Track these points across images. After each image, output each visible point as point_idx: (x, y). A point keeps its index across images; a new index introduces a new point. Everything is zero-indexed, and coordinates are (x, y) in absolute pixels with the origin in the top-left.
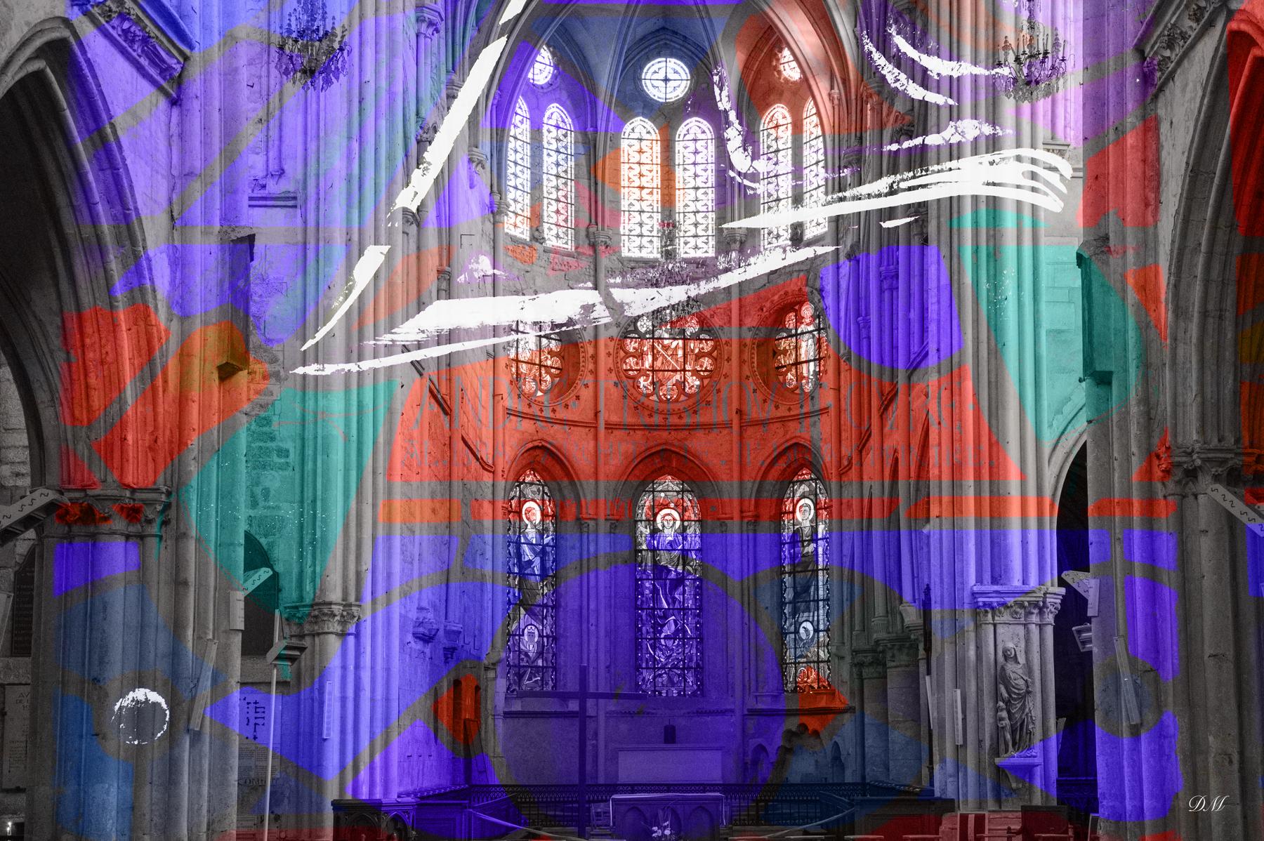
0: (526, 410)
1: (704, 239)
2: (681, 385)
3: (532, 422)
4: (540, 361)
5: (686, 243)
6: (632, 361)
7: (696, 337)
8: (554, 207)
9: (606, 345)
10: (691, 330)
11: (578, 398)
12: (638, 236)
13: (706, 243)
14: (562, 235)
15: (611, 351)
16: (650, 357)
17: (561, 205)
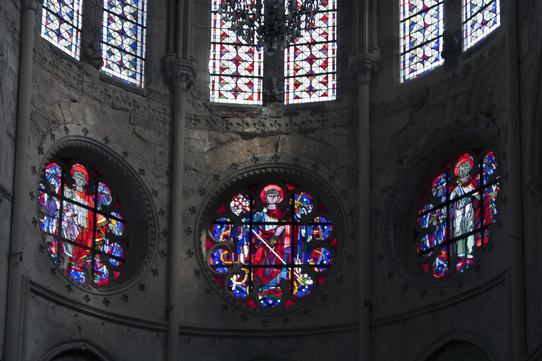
0: (64, 292)
1: (321, 78)
2: (290, 282)
3: (73, 313)
4: (94, 242)
5: (297, 85)
6: (222, 254)
7: (308, 221)
8: (117, 25)
9: (185, 219)
10: (304, 211)
11: (142, 287)
12: (232, 76)
13: (325, 83)
14: (127, 65)
15: (192, 228)
16: (246, 249)
17: (127, 25)
